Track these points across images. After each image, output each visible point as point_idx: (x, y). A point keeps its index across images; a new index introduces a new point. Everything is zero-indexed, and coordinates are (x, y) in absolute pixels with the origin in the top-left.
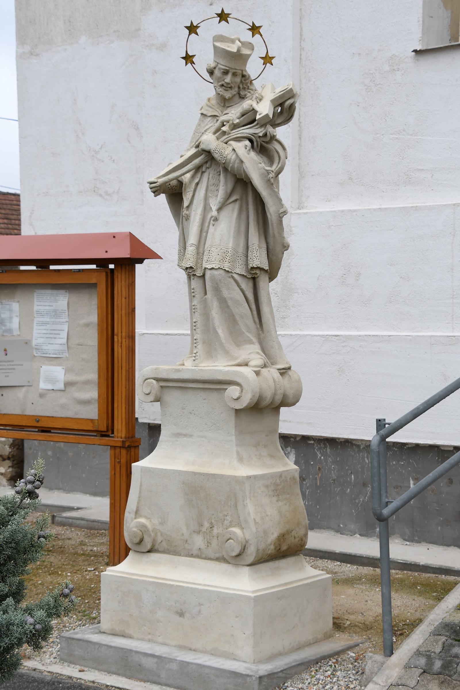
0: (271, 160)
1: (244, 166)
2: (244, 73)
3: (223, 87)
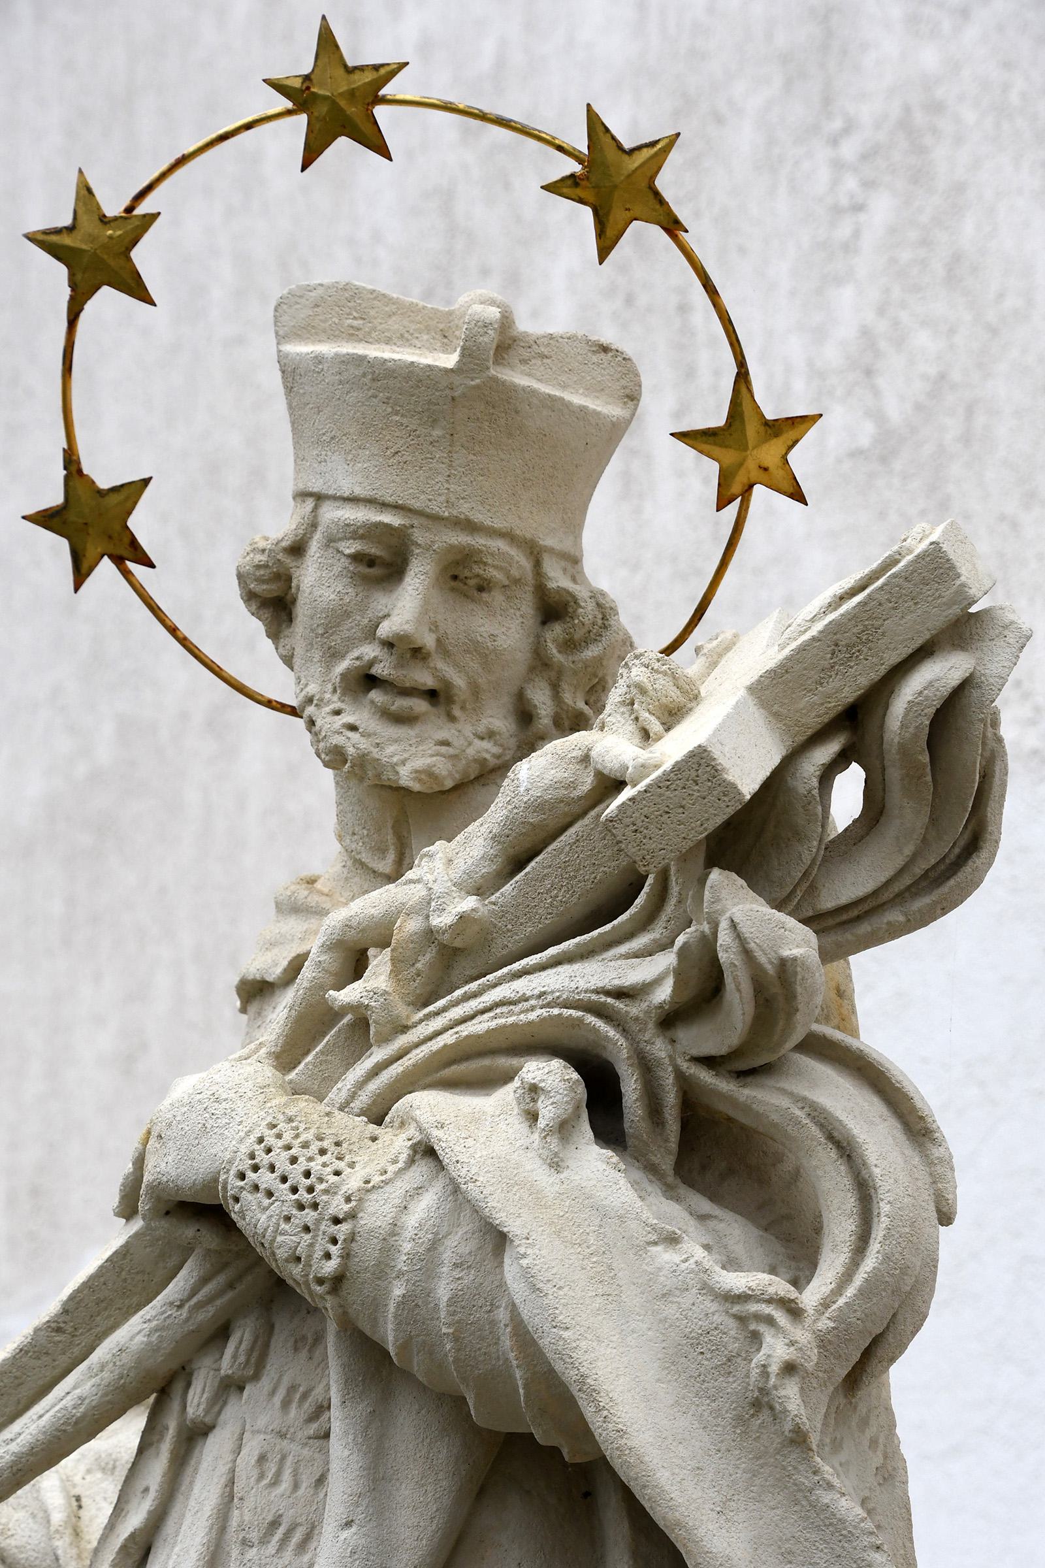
0: (793, 1241)
1: (517, 1288)
2: (557, 578)
3: (376, 695)
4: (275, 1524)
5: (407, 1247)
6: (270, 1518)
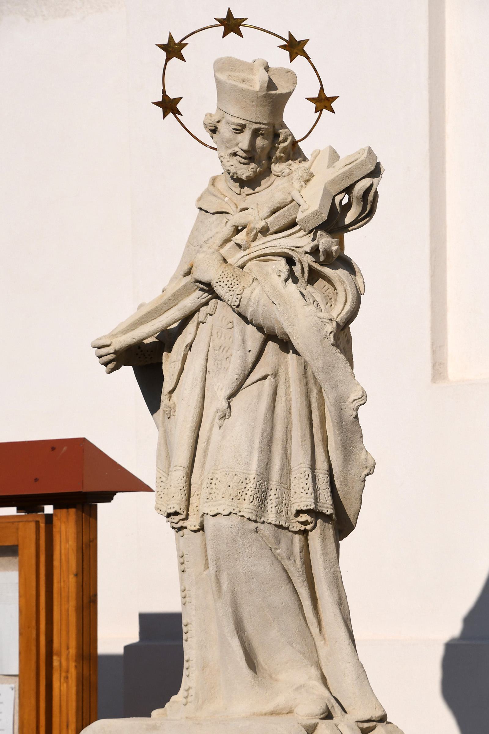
5: (253, 301)
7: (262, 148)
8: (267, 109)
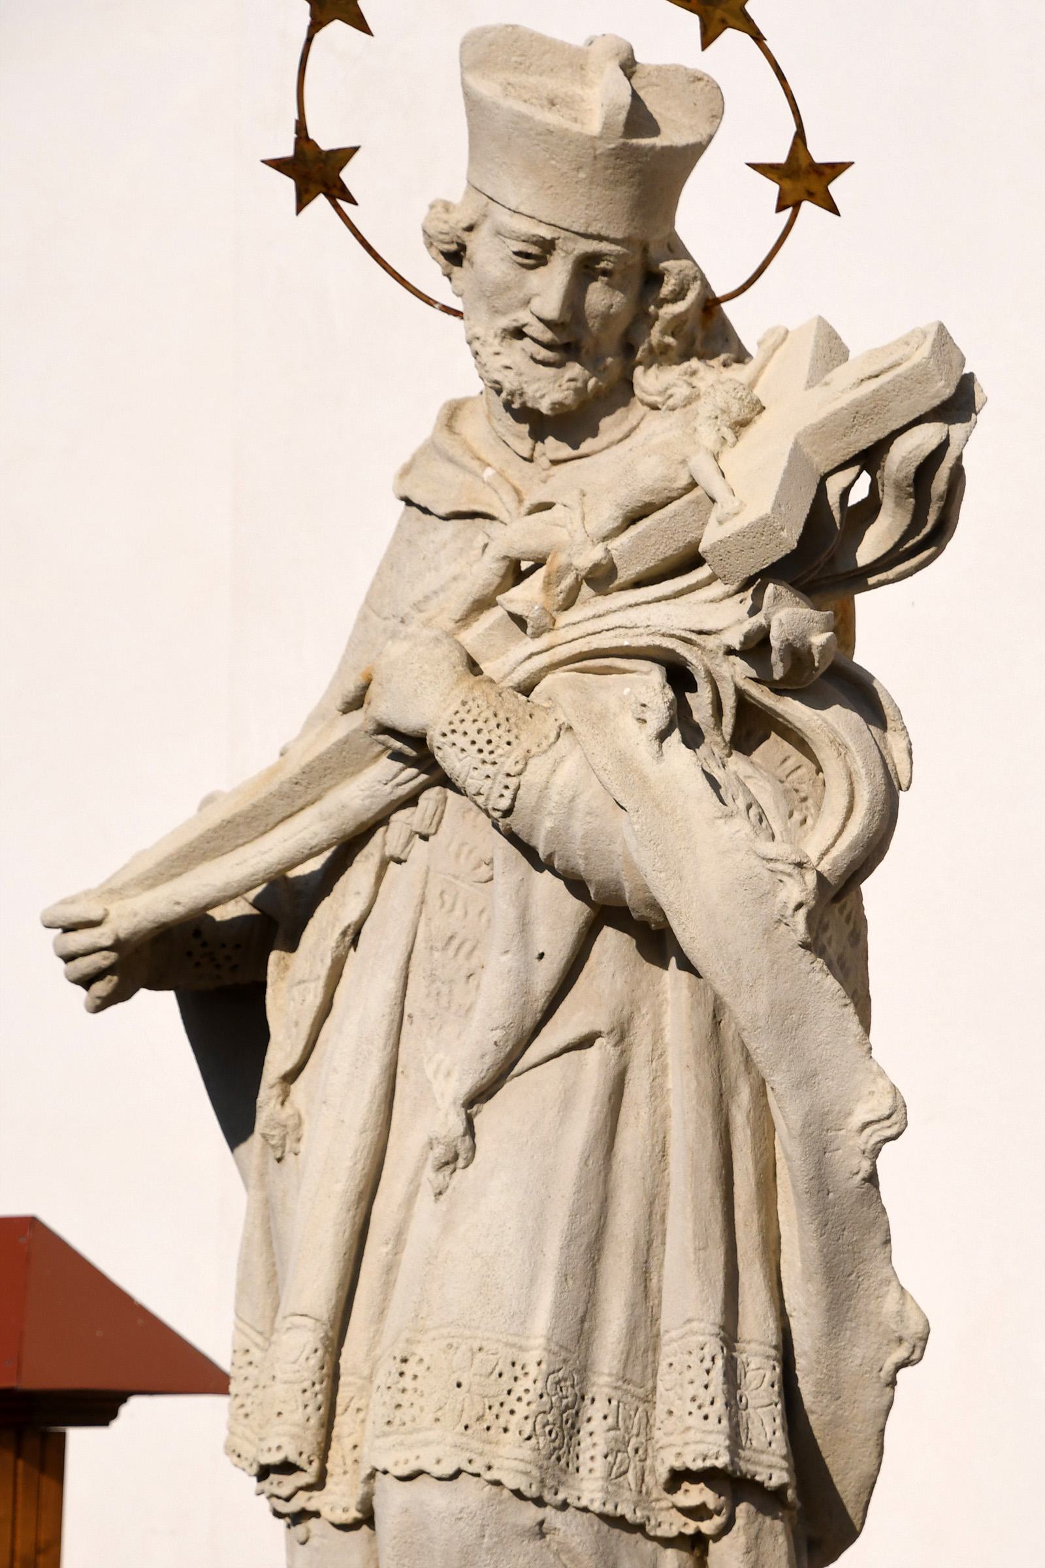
4: (451, 938)
5: (556, 798)
6: (449, 934)
7: (607, 318)
8: (624, 193)
